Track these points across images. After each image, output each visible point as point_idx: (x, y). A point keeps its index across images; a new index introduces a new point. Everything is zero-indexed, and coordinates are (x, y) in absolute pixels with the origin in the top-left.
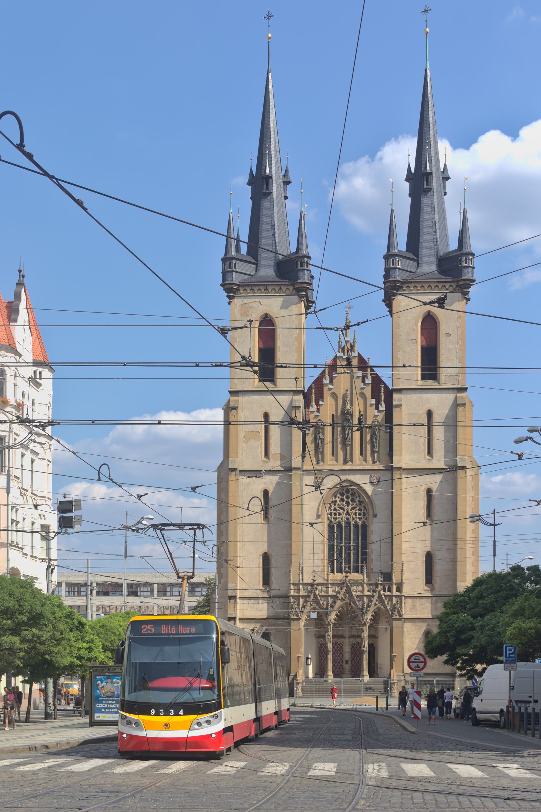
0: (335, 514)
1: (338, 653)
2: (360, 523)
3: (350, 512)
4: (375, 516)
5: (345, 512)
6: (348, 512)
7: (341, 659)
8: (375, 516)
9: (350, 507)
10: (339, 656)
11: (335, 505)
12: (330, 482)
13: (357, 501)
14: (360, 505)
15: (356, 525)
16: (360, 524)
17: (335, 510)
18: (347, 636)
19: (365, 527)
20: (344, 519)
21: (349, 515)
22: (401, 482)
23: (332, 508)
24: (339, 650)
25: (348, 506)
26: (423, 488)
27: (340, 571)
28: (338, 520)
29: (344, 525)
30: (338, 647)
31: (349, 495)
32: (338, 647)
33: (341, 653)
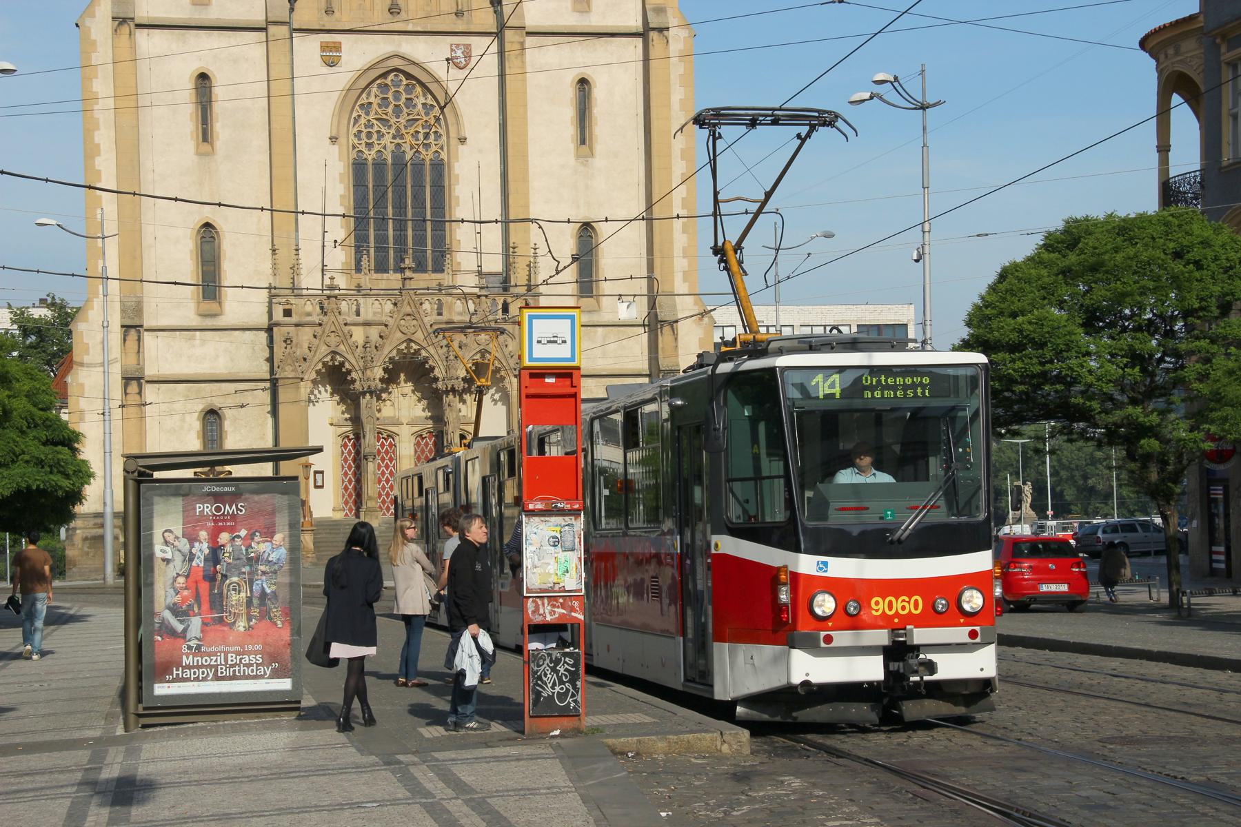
0: (369, 135)
1: (383, 459)
2: (427, 155)
3: (404, 131)
4: (462, 140)
5: (392, 131)
6: (398, 130)
7: (391, 474)
8: (462, 140)
9: (402, 120)
10: (387, 467)
11: (367, 114)
12: (360, 54)
13: (420, 106)
14: (427, 114)
15: (418, 166)
16: (428, 162)
17: (369, 125)
18: (405, 421)
19: (439, 168)
20: (391, 147)
21: (402, 136)
22: (523, 62)
23: (363, 121)
24: (387, 452)
25: (398, 117)
26: (571, 78)
27: (381, 268)
28: (377, 148)
29: (390, 161)
30: (383, 445)
31: (401, 89)
32: (383, 445)
33: (391, 460)
